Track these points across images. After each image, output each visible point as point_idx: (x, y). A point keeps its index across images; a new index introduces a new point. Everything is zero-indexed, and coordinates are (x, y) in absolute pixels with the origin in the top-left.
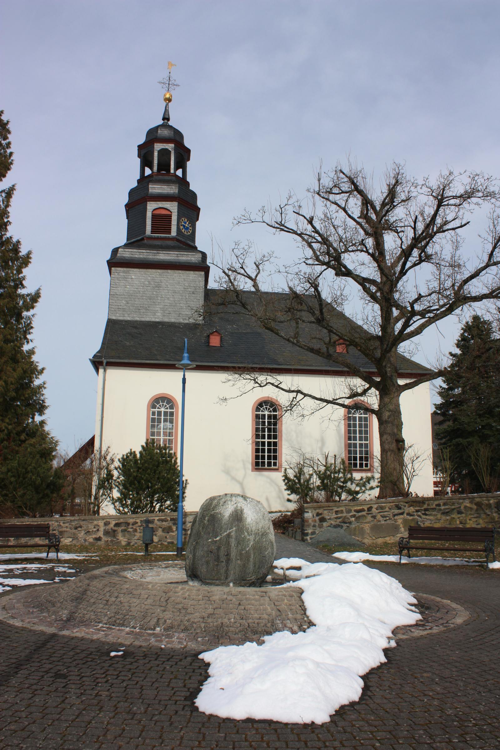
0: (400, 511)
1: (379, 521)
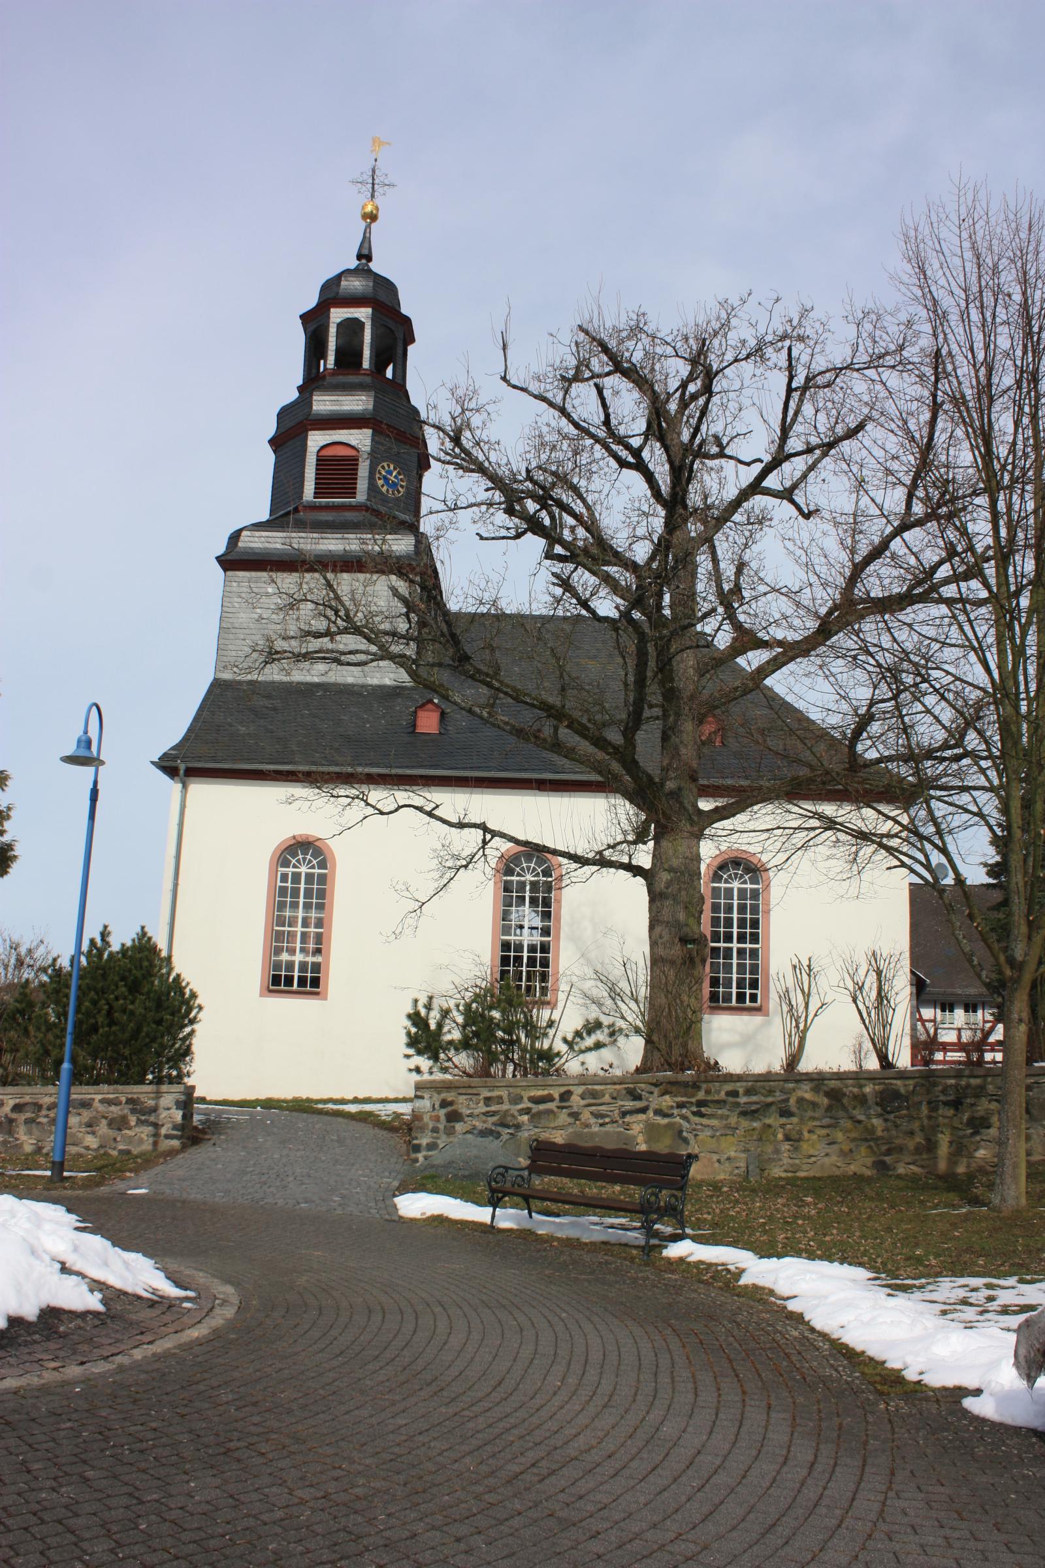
0: (639, 1104)
1: (588, 1126)
